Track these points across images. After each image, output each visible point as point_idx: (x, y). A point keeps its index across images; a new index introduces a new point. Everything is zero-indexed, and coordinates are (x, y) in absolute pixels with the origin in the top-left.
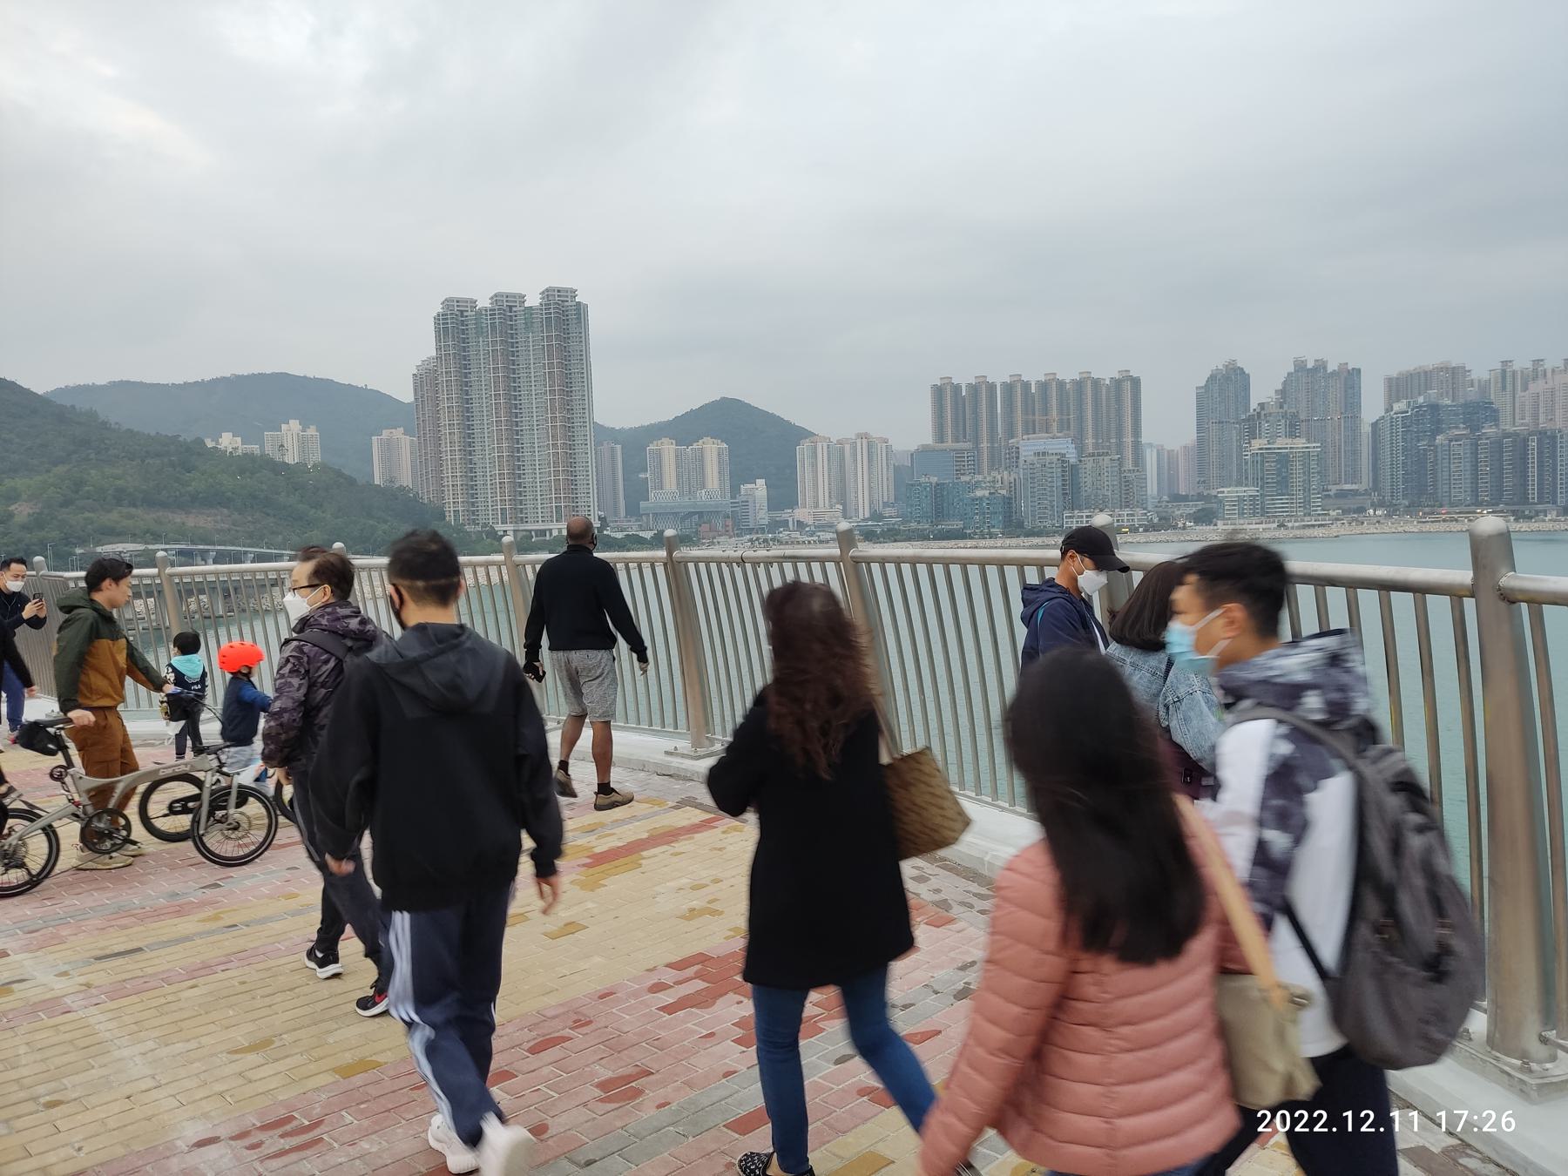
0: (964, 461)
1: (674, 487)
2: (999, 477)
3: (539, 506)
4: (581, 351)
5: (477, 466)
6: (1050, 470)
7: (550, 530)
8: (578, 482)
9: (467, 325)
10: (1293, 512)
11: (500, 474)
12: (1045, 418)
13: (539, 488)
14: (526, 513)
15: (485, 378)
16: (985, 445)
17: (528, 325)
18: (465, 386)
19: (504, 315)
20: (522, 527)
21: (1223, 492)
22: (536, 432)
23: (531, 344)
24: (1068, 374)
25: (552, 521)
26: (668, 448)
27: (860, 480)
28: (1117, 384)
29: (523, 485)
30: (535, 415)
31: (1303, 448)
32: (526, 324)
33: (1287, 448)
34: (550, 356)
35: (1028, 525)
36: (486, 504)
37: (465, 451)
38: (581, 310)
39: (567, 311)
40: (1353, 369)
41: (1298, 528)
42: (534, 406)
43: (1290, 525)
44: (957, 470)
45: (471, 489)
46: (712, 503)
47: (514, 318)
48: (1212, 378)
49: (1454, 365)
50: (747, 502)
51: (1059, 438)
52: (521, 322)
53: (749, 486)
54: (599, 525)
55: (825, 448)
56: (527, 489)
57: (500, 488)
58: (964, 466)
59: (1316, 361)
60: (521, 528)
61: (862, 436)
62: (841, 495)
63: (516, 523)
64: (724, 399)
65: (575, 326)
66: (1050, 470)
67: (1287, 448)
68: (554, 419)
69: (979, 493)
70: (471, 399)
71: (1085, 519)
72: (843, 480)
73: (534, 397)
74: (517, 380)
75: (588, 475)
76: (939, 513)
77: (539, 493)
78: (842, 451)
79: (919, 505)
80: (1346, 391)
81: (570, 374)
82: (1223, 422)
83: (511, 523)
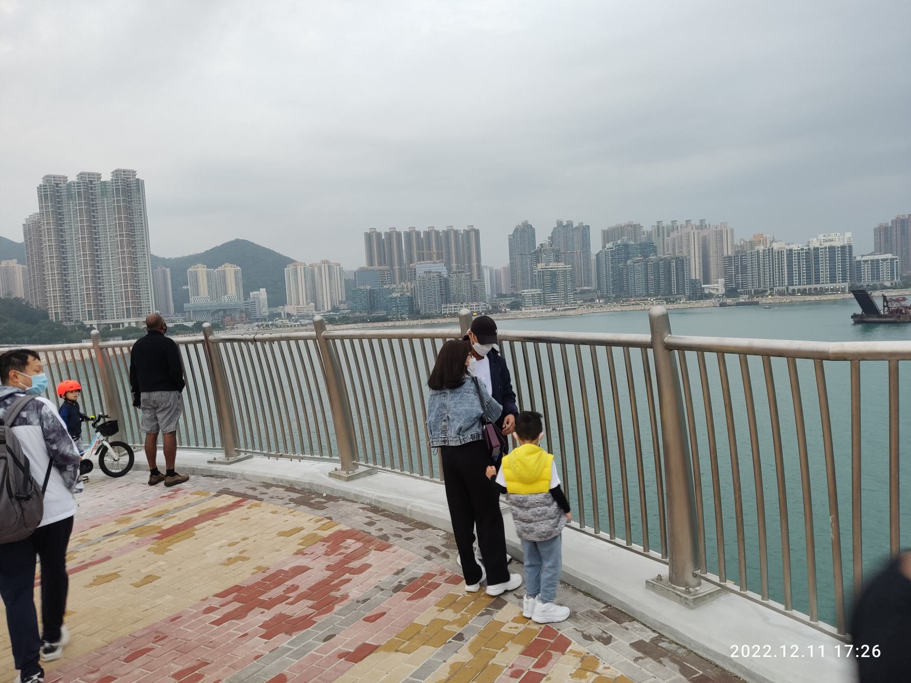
1: (206, 294)
2: (405, 286)
3: (115, 308)
5: (71, 283)
6: (433, 281)
7: (123, 324)
8: (141, 293)
9: (61, 193)
10: (559, 302)
11: (86, 288)
12: (429, 252)
13: (114, 297)
14: (106, 313)
15: (75, 226)
16: (396, 267)
17: (104, 193)
18: (60, 232)
19: (87, 186)
20: (103, 322)
21: (524, 292)
23: (106, 205)
24: (441, 227)
25: (124, 318)
26: (201, 270)
27: (324, 289)
28: (467, 232)
29: (103, 295)
30: (110, 250)
31: (563, 268)
32: (102, 192)
33: (555, 268)
34: (119, 213)
35: (422, 312)
36: (77, 308)
37: (61, 273)
38: (139, 184)
40: (586, 226)
41: (562, 310)
42: (109, 244)
43: (558, 309)
44: (381, 282)
45: (66, 298)
46: (233, 303)
48: (516, 230)
49: (635, 224)
51: (438, 263)
52: (98, 191)
53: (255, 293)
56: (106, 298)
57: (87, 297)
59: (567, 221)
60: (102, 323)
61: (324, 262)
62: (314, 297)
63: (99, 319)
64: (237, 241)
65: (136, 194)
66: (433, 281)
67: (555, 268)
68: (123, 252)
69: (394, 295)
70: (65, 240)
71: (453, 309)
72: (314, 288)
73: (109, 238)
74: (97, 228)
75: (148, 288)
76: (372, 307)
77: (114, 300)
78: (313, 271)
79: (361, 302)
80: (583, 237)
81: (134, 224)
82: (522, 254)
83: (95, 319)
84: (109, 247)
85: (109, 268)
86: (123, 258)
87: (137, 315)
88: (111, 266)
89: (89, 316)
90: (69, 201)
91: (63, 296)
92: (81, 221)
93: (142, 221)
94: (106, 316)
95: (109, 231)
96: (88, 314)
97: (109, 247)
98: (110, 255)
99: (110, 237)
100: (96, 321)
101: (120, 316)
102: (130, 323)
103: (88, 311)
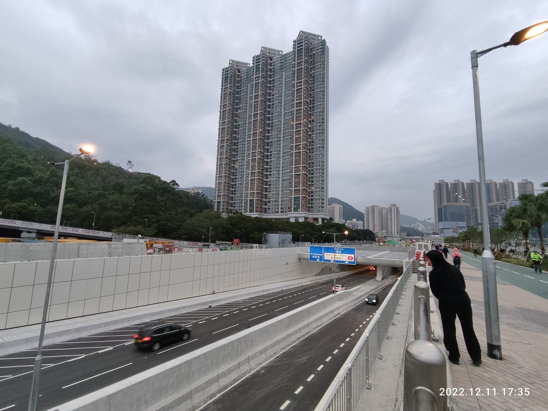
0: (470, 211)
3: (280, 200)
4: (324, 74)
5: (238, 171)
8: (314, 179)
13: (281, 186)
22: (282, 142)
25: (290, 211)
39: (314, 48)
42: (282, 123)
47: (273, 64)
50: (355, 226)
52: (278, 65)
53: (350, 221)
54: (328, 218)
55: (378, 209)
58: (470, 213)
61: (394, 205)
63: (261, 212)
72: (382, 222)
77: (280, 189)
78: (382, 211)
83: (257, 211)
84: (282, 126)
87: (307, 208)
88: (282, 149)
91: (228, 183)
93: (324, 88)
95: (284, 108)
96: (250, 204)
97: (282, 126)
98: (282, 136)
99: (284, 115)
100: (257, 213)
101: (285, 210)
102: (297, 218)
103: (251, 200)
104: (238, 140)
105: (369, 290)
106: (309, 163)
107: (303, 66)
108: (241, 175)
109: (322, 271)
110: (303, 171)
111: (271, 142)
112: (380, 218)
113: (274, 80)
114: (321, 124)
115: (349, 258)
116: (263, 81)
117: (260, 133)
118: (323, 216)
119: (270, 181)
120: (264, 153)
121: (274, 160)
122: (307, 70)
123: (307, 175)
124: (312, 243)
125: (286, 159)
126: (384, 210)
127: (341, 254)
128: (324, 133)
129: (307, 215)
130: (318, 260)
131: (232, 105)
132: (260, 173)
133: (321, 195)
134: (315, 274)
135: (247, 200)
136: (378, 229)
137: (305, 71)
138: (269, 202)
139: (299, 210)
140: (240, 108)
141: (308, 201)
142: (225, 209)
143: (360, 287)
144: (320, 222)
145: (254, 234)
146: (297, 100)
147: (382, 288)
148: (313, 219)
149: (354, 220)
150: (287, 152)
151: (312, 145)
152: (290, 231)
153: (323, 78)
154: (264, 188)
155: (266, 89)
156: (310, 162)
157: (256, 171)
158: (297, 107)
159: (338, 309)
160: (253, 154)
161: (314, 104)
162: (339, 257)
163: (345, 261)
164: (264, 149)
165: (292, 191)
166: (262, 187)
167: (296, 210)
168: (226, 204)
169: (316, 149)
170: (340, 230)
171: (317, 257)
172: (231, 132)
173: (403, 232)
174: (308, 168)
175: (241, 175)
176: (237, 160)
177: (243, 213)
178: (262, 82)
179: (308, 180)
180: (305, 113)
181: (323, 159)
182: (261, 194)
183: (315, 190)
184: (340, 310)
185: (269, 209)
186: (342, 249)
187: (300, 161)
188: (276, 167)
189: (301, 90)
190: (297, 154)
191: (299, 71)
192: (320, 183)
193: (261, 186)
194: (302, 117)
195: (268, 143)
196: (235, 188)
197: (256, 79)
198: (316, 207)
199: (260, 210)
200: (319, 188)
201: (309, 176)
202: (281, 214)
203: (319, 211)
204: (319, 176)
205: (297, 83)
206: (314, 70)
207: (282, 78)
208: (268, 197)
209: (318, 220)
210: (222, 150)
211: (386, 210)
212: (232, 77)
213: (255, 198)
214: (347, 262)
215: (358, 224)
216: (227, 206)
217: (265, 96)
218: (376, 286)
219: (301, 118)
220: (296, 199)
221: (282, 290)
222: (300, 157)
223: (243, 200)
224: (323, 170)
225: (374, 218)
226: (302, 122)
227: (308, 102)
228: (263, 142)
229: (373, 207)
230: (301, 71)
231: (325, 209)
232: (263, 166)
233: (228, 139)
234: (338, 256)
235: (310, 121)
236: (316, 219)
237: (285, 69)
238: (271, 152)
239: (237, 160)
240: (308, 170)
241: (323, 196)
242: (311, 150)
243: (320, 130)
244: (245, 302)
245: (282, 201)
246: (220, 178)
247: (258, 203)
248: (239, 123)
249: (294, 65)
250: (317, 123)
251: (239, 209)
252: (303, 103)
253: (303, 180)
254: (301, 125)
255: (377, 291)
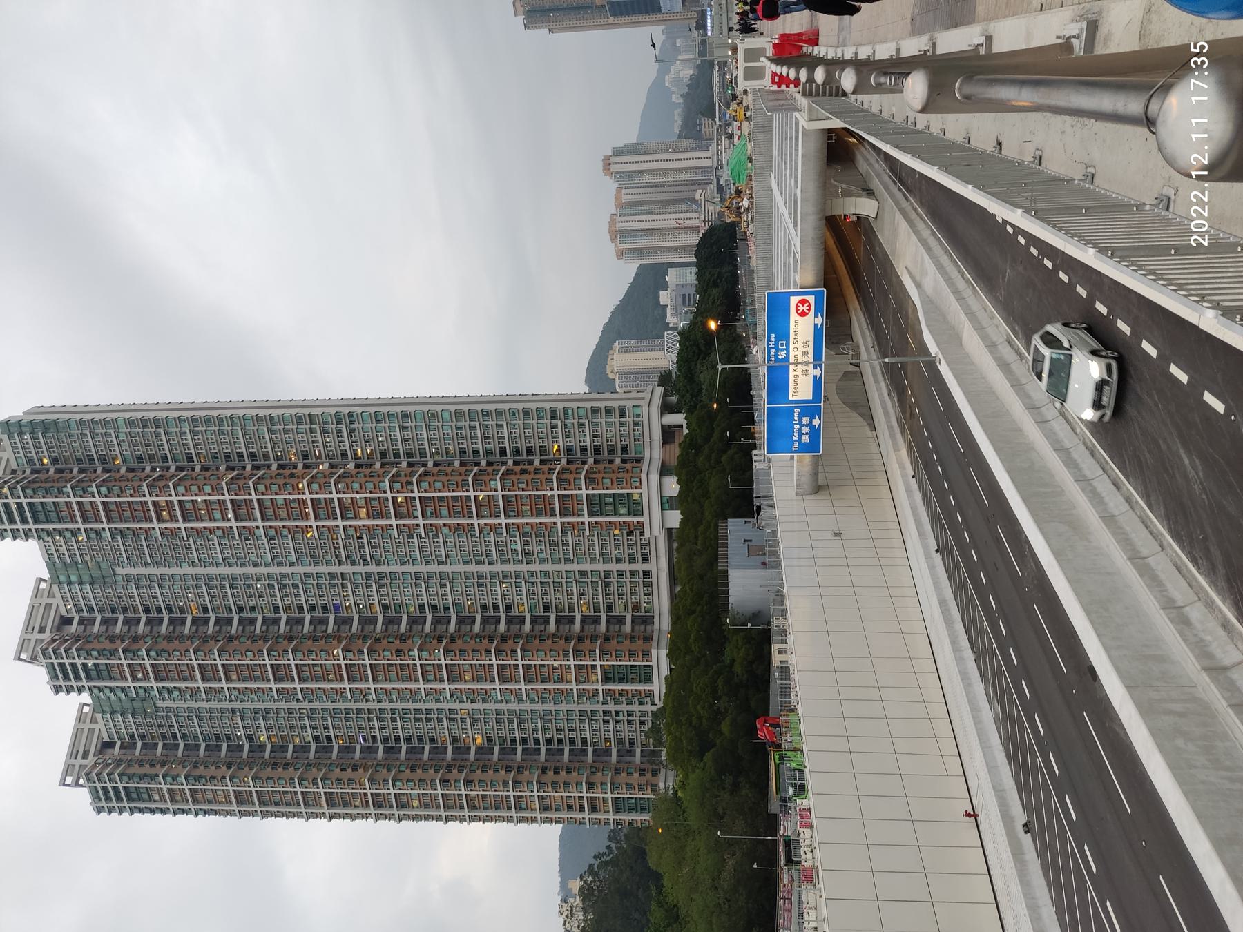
3: (601, 567)
4: (130, 422)
8: (522, 443)
9: (132, 736)
13: (548, 567)
22: (384, 569)
25: (640, 527)
30: (336, 569)
47: (86, 614)
53: (669, 315)
54: (659, 391)
61: (607, 163)
63: (647, 639)
70: (317, 739)
73: (286, 570)
77: (562, 567)
78: (629, 204)
83: (647, 654)
85: (418, 576)
86: (347, 510)
87: (628, 466)
88: (409, 568)
89: (633, 681)
90: (157, 709)
91: (544, 770)
92: (208, 674)
93: (180, 421)
94: (635, 607)
95: (255, 564)
96: (621, 681)
98: (360, 569)
99: (280, 564)
100: (654, 652)
101: (637, 549)
102: (667, 504)
103: (606, 680)
104: (374, 737)
105: (914, 238)
106: (462, 464)
107: (98, 500)
108: (510, 721)
109: (854, 406)
110: (493, 486)
111: (385, 608)
112: (652, 209)
113: (147, 610)
114: (316, 426)
115: (803, 314)
116: (148, 651)
117: (350, 655)
118: (656, 409)
119: (532, 607)
120: (427, 635)
121: (453, 595)
122: (113, 483)
123: (508, 472)
124: (754, 447)
125: (447, 551)
126: (625, 198)
127: (792, 340)
128: (350, 415)
129: (651, 468)
130: (816, 422)
131: (239, 768)
132: (503, 646)
133: (580, 417)
134: (867, 428)
135: (606, 694)
136: (696, 215)
137: (116, 490)
138: (610, 607)
139: (636, 497)
140: (250, 738)
141: (601, 466)
142: (643, 780)
143: (905, 271)
144: (678, 418)
145: (733, 661)
146: (224, 518)
147: (904, 195)
148: (668, 446)
149: (665, 298)
150: (421, 547)
151: (397, 455)
152: (717, 526)
153: (144, 423)
154: (557, 630)
155: (181, 637)
156: (457, 464)
157: (494, 662)
158: (251, 518)
159: (991, 346)
160: (430, 678)
161: (240, 455)
162: (801, 350)
163: (816, 325)
164: (409, 635)
165: (568, 523)
166: (554, 636)
167: (635, 508)
168: (624, 775)
169: (411, 442)
170: (703, 348)
171: (807, 426)
172: (343, 770)
173: (701, 130)
174: (480, 470)
175: (510, 721)
176: (454, 740)
177: (654, 708)
178: (153, 654)
179: (526, 467)
180: (275, 487)
181: (446, 415)
182: (581, 639)
183: (560, 439)
184: (995, 339)
185: (635, 607)
186: (773, 340)
187: (454, 498)
188: (480, 585)
189: (189, 506)
190: (429, 509)
191: (115, 514)
192: (535, 422)
193: (549, 642)
194: (291, 497)
195: (389, 621)
196: (560, 741)
197: (140, 676)
198: (621, 435)
199: (640, 642)
200: (554, 426)
201: (510, 463)
202: (654, 559)
203: (636, 424)
204: (511, 427)
205: (160, 519)
206: (114, 460)
207: (139, 576)
208: (592, 614)
209: (670, 426)
210: (415, 803)
211: (624, 191)
212: (130, 771)
213: (598, 663)
214: (819, 320)
215: (677, 285)
216: (629, 774)
217: (206, 642)
218: (899, 216)
219: (294, 500)
220: (596, 506)
221: (937, 551)
222: (440, 498)
223: (606, 708)
224: (486, 414)
225: (653, 229)
226: (307, 497)
227: (232, 478)
228: (384, 642)
229: (616, 235)
230: (113, 507)
231: (629, 404)
232: (477, 636)
233: (372, 781)
234: (799, 353)
235: (306, 467)
236: (668, 434)
237: (104, 566)
238: (422, 608)
239: (454, 740)
240: (490, 469)
241: (582, 412)
242: (415, 460)
243: (339, 431)
244: (997, 692)
245: (606, 559)
246: (524, 806)
247: (616, 651)
248: (310, 739)
249: (93, 535)
250: (313, 442)
251: (642, 723)
252: (236, 494)
253: (525, 487)
254: (319, 499)
255: (915, 210)
